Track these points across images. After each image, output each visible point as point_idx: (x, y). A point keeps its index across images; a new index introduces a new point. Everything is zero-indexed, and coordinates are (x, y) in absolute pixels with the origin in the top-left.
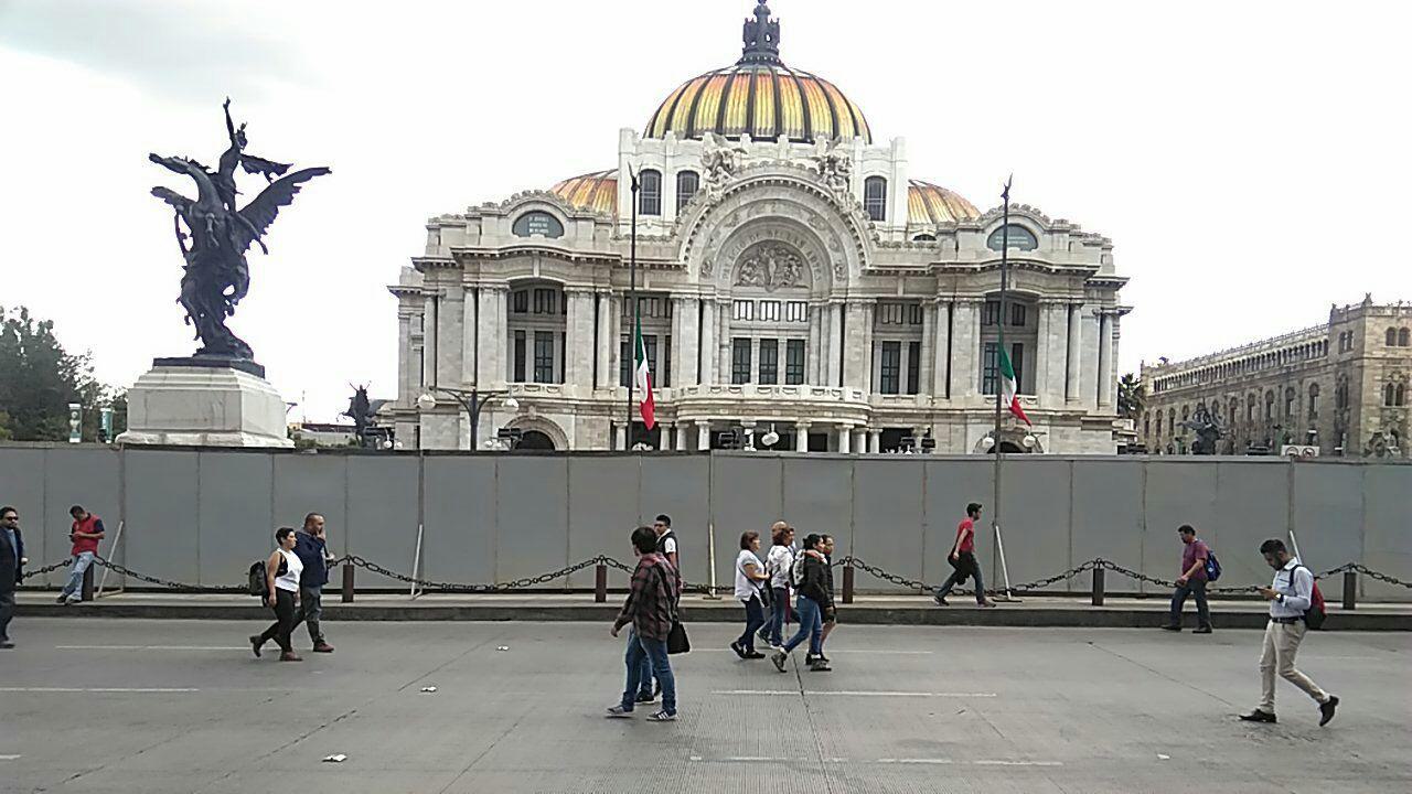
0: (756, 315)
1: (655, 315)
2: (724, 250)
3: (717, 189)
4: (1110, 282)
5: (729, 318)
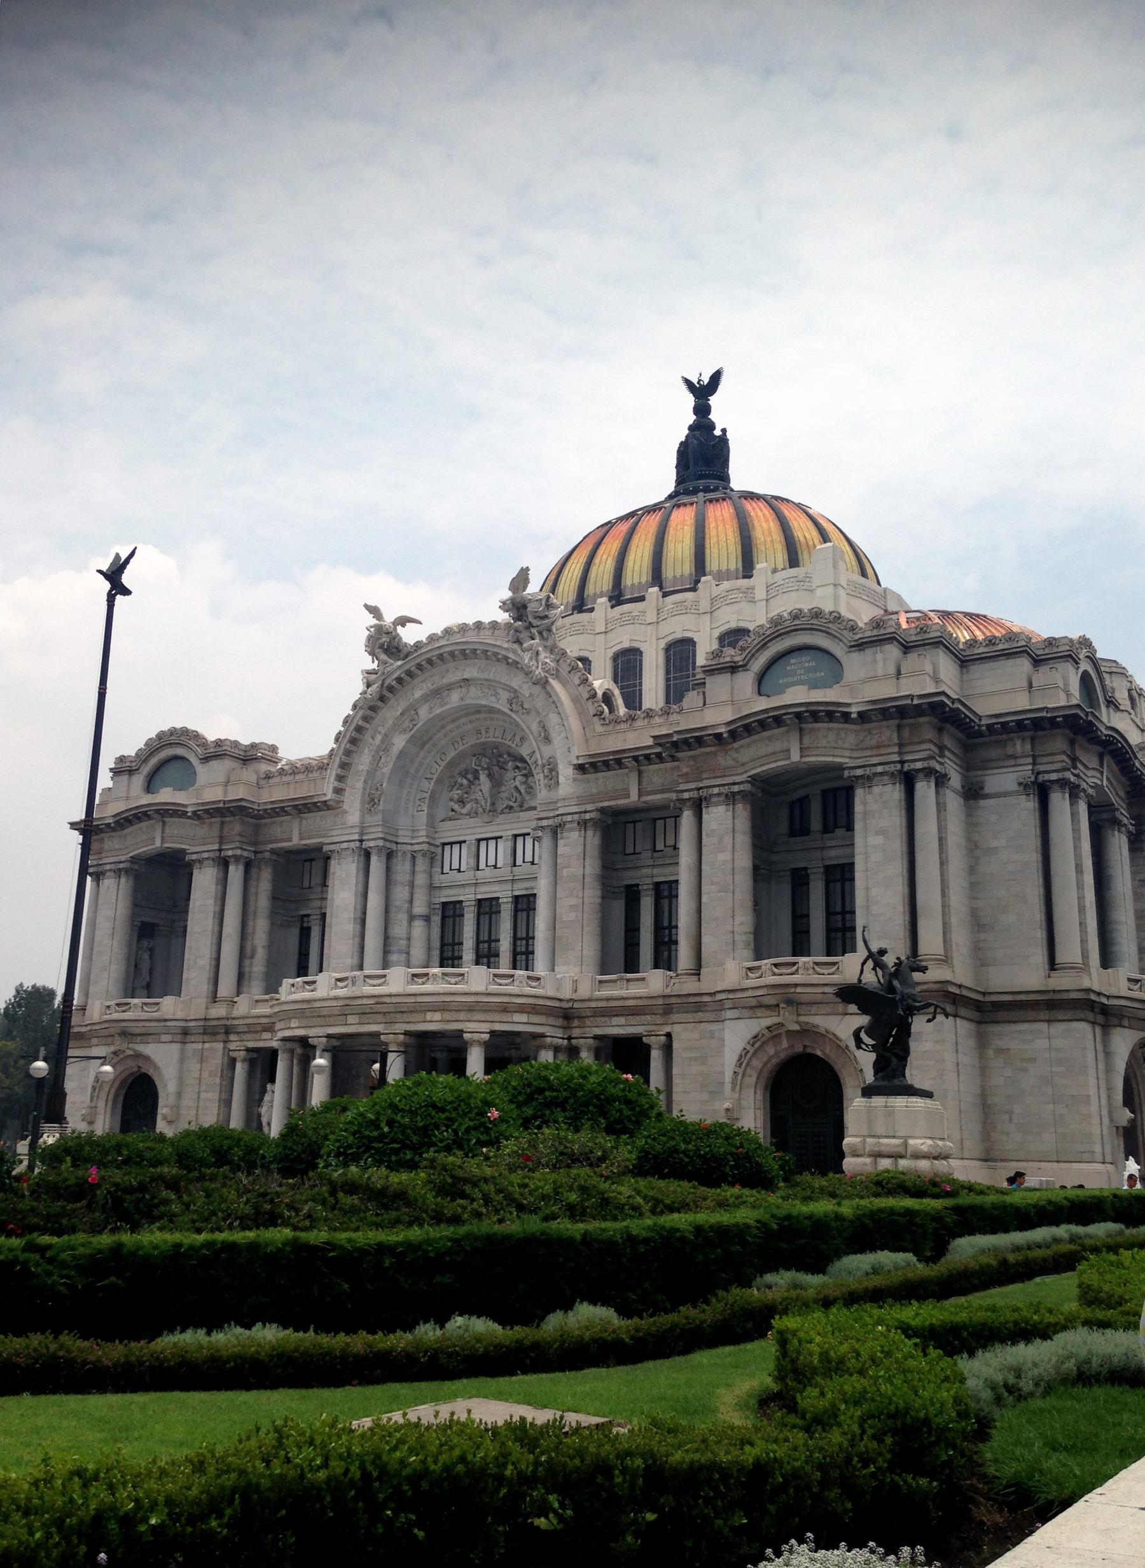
2: (412, 771)
4: (1034, 720)
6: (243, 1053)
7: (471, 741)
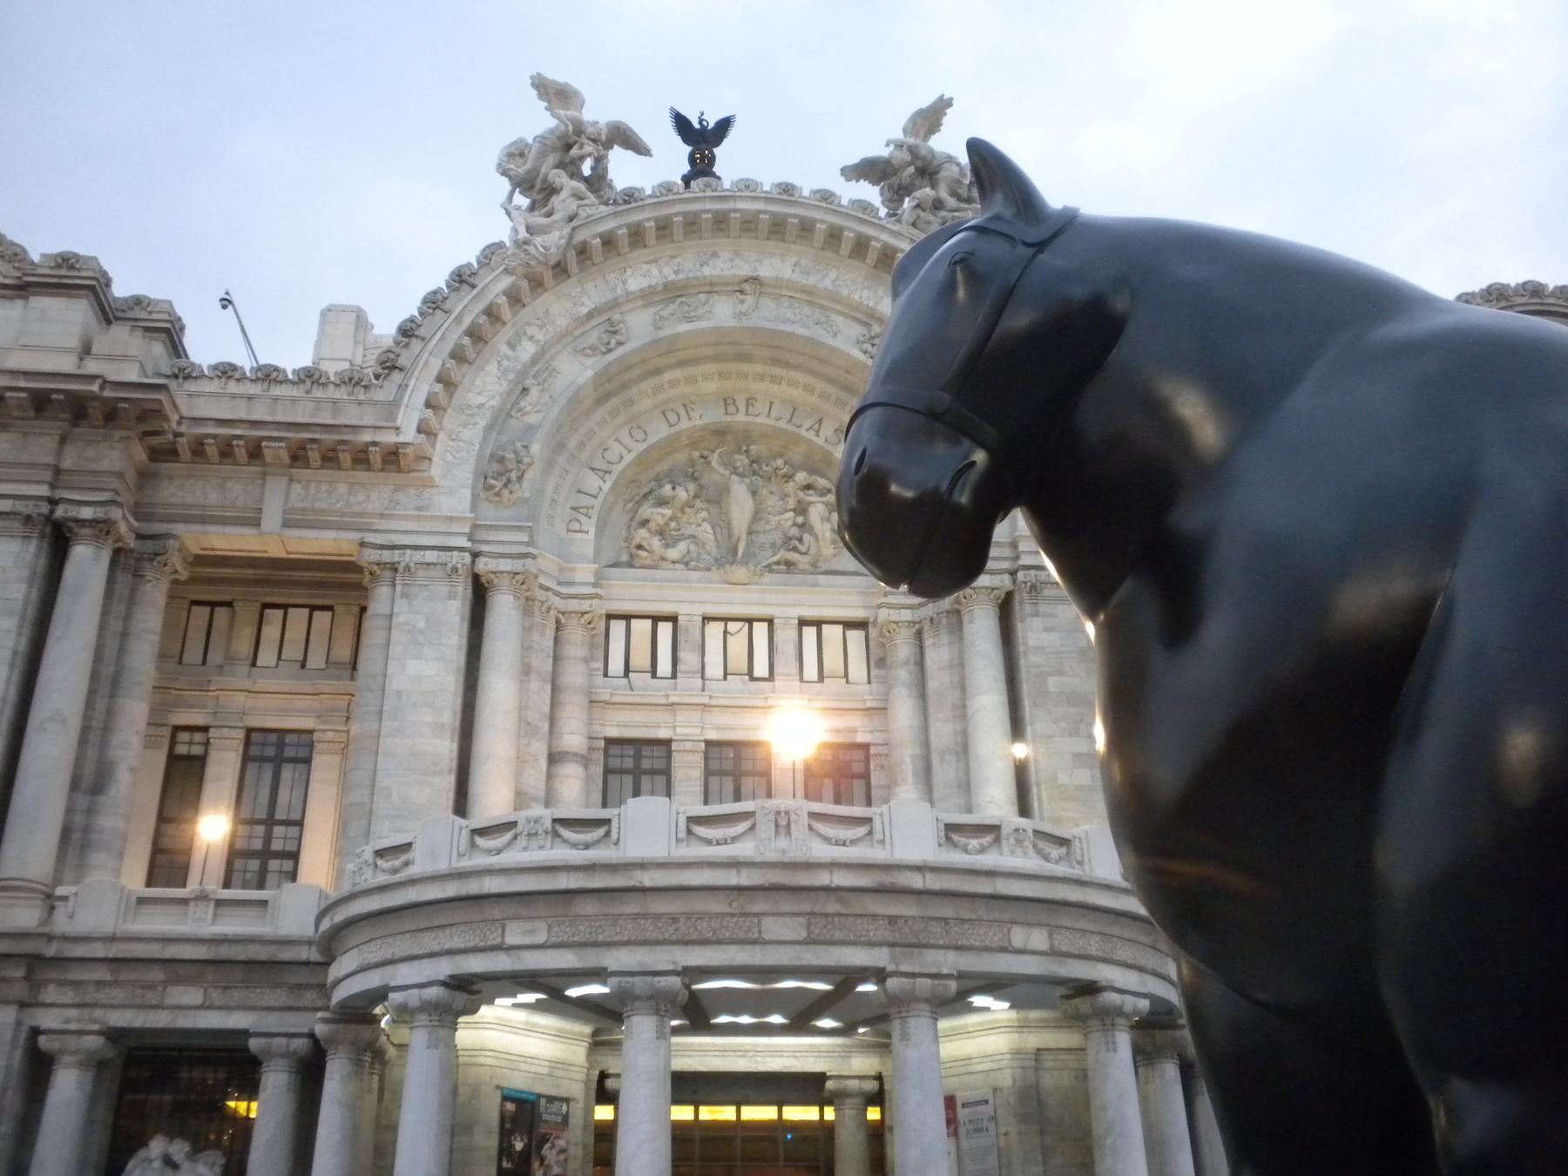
0: (688, 658)
1: (316, 660)
2: (572, 444)
3: (544, 230)
5: (590, 674)
6: (93, 1042)
7: (713, 416)
